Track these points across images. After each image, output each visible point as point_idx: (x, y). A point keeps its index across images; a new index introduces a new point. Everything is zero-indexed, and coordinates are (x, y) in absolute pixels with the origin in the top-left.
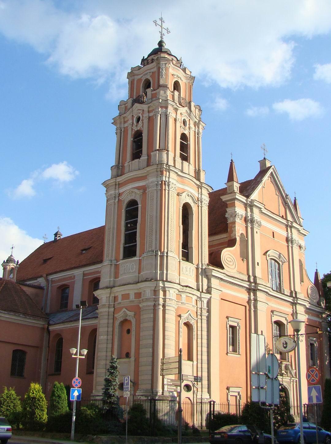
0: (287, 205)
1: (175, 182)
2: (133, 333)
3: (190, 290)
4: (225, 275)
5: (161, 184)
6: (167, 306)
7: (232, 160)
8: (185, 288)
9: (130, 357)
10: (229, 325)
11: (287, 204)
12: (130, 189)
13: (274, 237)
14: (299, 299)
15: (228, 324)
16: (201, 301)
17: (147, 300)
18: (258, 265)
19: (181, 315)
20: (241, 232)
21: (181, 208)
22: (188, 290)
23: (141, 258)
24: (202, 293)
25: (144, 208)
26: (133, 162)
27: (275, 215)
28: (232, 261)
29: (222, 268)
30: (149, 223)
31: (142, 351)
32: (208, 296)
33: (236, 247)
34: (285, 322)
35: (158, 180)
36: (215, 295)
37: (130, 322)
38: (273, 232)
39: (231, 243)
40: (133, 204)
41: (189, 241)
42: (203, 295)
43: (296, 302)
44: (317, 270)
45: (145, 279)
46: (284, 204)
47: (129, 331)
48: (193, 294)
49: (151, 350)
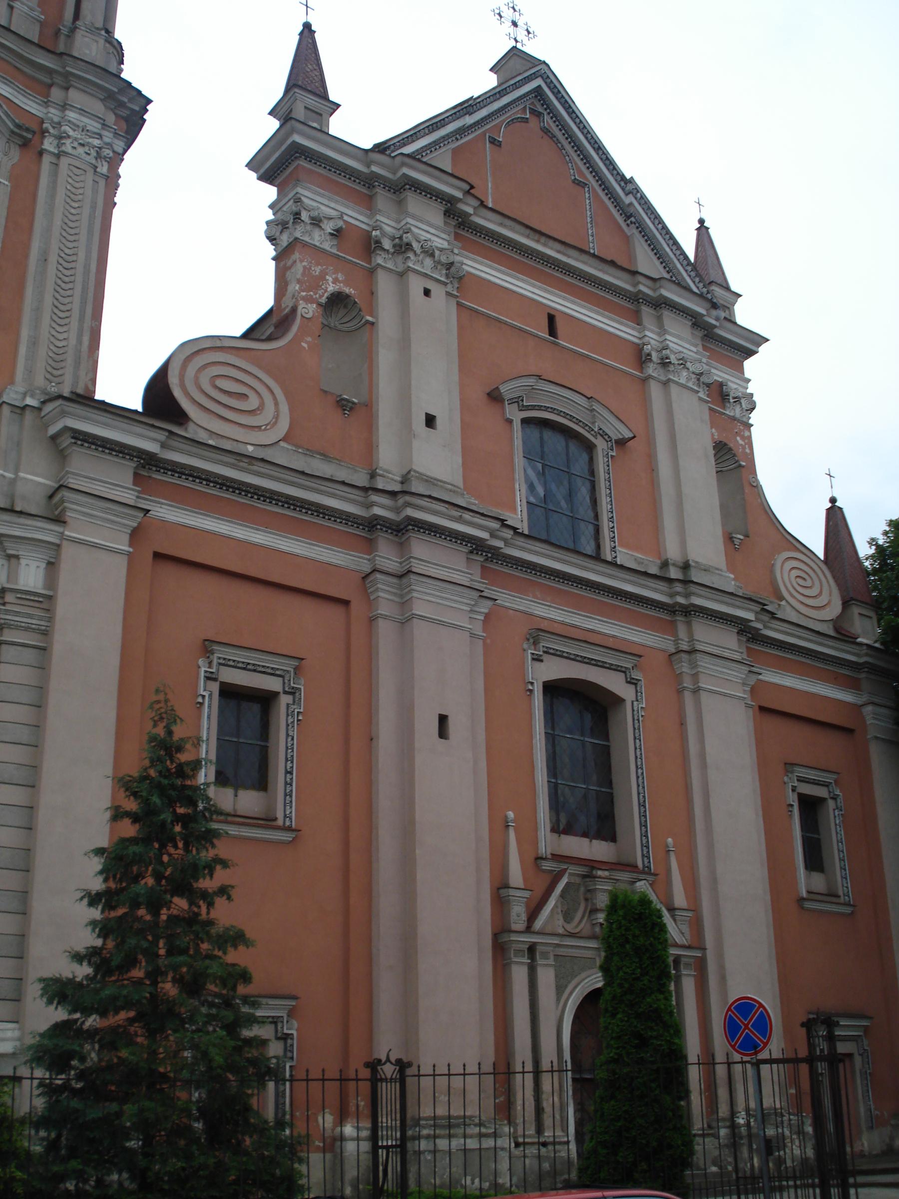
0: (633, 219)
7: (307, 26)
10: (215, 687)
11: (631, 216)
13: (552, 331)
15: (210, 678)
18: (430, 421)
20: (331, 288)
27: (551, 243)
32: (47, 533)
33: (296, 340)
34: (625, 692)
38: (551, 319)
43: (681, 600)
44: (833, 500)
46: (620, 220)
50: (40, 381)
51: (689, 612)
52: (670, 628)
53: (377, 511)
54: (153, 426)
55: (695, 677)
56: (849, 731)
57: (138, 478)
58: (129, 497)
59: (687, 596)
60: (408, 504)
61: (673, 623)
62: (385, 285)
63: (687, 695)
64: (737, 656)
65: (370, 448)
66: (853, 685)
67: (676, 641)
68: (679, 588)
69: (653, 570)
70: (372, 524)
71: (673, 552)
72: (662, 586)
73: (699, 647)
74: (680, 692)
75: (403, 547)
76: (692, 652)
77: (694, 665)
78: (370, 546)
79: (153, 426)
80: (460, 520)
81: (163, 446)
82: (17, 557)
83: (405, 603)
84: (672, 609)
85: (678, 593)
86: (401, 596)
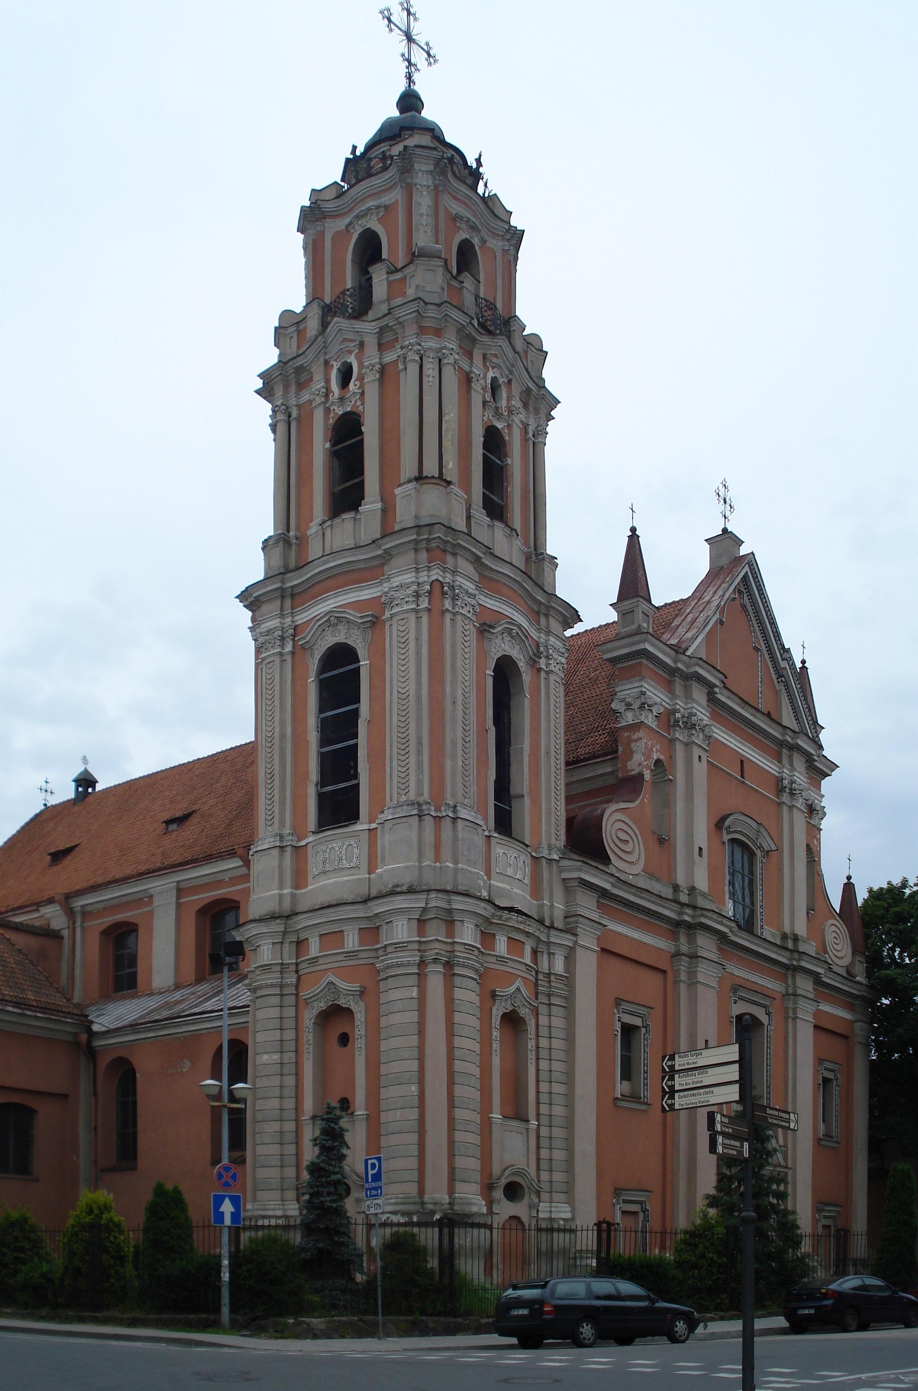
1: (470, 586)
2: (359, 1043)
3: (520, 919)
4: (612, 880)
5: (430, 592)
6: (458, 965)
8: (505, 914)
9: (350, 1112)
12: (330, 612)
14: (804, 957)
16: (549, 954)
17: (400, 947)
19: (495, 991)
21: (490, 672)
22: (514, 920)
23: (374, 826)
24: (553, 932)
25: (378, 670)
26: (337, 521)
28: (629, 839)
29: (606, 860)
30: (395, 717)
31: (389, 1093)
32: (567, 940)
35: (421, 580)
36: (588, 940)
37: (349, 1012)
39: (631, 785)
40: (341, 655)
41: (511, 777)
42: (555, 937)
43: (795, 963)
45: (390, 886)
47: (344, 1039)
48: (528, 934)
49: (414, 1088)
50: (553, 841)
51: (796, 969)
52: (783, 978)
53: (686, 918)
54: (597, 868)
55: (795, 1010)
56: (846, 1037)
57: (600, 905)
58: (595, 916)
59: (799, 960)
60: (702, 915)
61: (786, 975)
62: (679, 750)
63: (790, 1020)
64: (811, 996)
65: (672, 869)
66: (850, 1008)
67: (787, 988)
68: (796, 956)
69: (778, 942)
70: (678, 924)
71: (787, 929)
72: (787, 954)
73: (799, 992)
74: (786, 1019)
75: (691, 939)
76: (795, 995)
77: (795, 1003)
78: (674, 937)
79: (597, 868)
80: (721, 923)
81: (613, 885)
82: (553, 954)
83: (692, 974)
84: (787, 967)
85: (795, 959)
86: (689, 968)
